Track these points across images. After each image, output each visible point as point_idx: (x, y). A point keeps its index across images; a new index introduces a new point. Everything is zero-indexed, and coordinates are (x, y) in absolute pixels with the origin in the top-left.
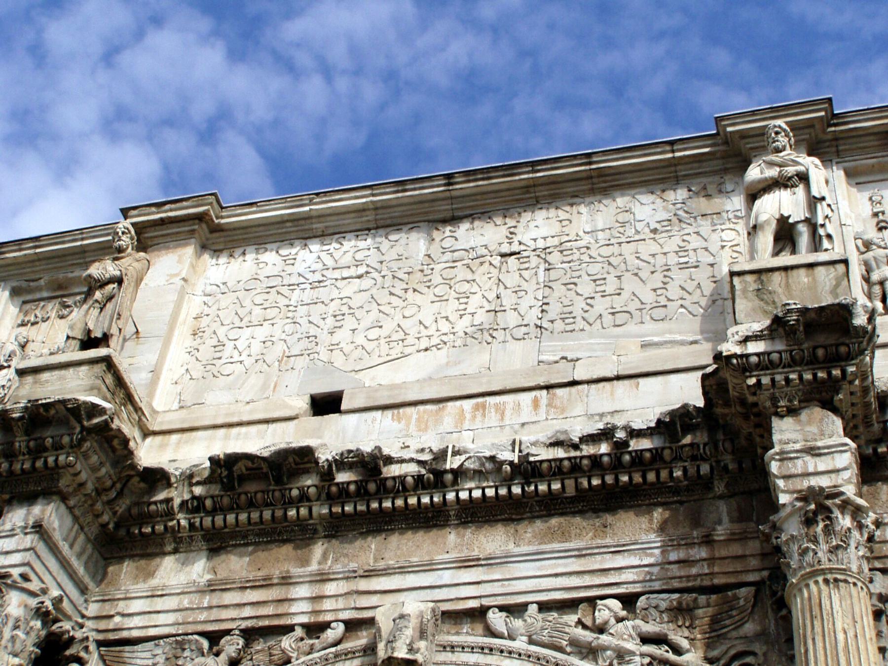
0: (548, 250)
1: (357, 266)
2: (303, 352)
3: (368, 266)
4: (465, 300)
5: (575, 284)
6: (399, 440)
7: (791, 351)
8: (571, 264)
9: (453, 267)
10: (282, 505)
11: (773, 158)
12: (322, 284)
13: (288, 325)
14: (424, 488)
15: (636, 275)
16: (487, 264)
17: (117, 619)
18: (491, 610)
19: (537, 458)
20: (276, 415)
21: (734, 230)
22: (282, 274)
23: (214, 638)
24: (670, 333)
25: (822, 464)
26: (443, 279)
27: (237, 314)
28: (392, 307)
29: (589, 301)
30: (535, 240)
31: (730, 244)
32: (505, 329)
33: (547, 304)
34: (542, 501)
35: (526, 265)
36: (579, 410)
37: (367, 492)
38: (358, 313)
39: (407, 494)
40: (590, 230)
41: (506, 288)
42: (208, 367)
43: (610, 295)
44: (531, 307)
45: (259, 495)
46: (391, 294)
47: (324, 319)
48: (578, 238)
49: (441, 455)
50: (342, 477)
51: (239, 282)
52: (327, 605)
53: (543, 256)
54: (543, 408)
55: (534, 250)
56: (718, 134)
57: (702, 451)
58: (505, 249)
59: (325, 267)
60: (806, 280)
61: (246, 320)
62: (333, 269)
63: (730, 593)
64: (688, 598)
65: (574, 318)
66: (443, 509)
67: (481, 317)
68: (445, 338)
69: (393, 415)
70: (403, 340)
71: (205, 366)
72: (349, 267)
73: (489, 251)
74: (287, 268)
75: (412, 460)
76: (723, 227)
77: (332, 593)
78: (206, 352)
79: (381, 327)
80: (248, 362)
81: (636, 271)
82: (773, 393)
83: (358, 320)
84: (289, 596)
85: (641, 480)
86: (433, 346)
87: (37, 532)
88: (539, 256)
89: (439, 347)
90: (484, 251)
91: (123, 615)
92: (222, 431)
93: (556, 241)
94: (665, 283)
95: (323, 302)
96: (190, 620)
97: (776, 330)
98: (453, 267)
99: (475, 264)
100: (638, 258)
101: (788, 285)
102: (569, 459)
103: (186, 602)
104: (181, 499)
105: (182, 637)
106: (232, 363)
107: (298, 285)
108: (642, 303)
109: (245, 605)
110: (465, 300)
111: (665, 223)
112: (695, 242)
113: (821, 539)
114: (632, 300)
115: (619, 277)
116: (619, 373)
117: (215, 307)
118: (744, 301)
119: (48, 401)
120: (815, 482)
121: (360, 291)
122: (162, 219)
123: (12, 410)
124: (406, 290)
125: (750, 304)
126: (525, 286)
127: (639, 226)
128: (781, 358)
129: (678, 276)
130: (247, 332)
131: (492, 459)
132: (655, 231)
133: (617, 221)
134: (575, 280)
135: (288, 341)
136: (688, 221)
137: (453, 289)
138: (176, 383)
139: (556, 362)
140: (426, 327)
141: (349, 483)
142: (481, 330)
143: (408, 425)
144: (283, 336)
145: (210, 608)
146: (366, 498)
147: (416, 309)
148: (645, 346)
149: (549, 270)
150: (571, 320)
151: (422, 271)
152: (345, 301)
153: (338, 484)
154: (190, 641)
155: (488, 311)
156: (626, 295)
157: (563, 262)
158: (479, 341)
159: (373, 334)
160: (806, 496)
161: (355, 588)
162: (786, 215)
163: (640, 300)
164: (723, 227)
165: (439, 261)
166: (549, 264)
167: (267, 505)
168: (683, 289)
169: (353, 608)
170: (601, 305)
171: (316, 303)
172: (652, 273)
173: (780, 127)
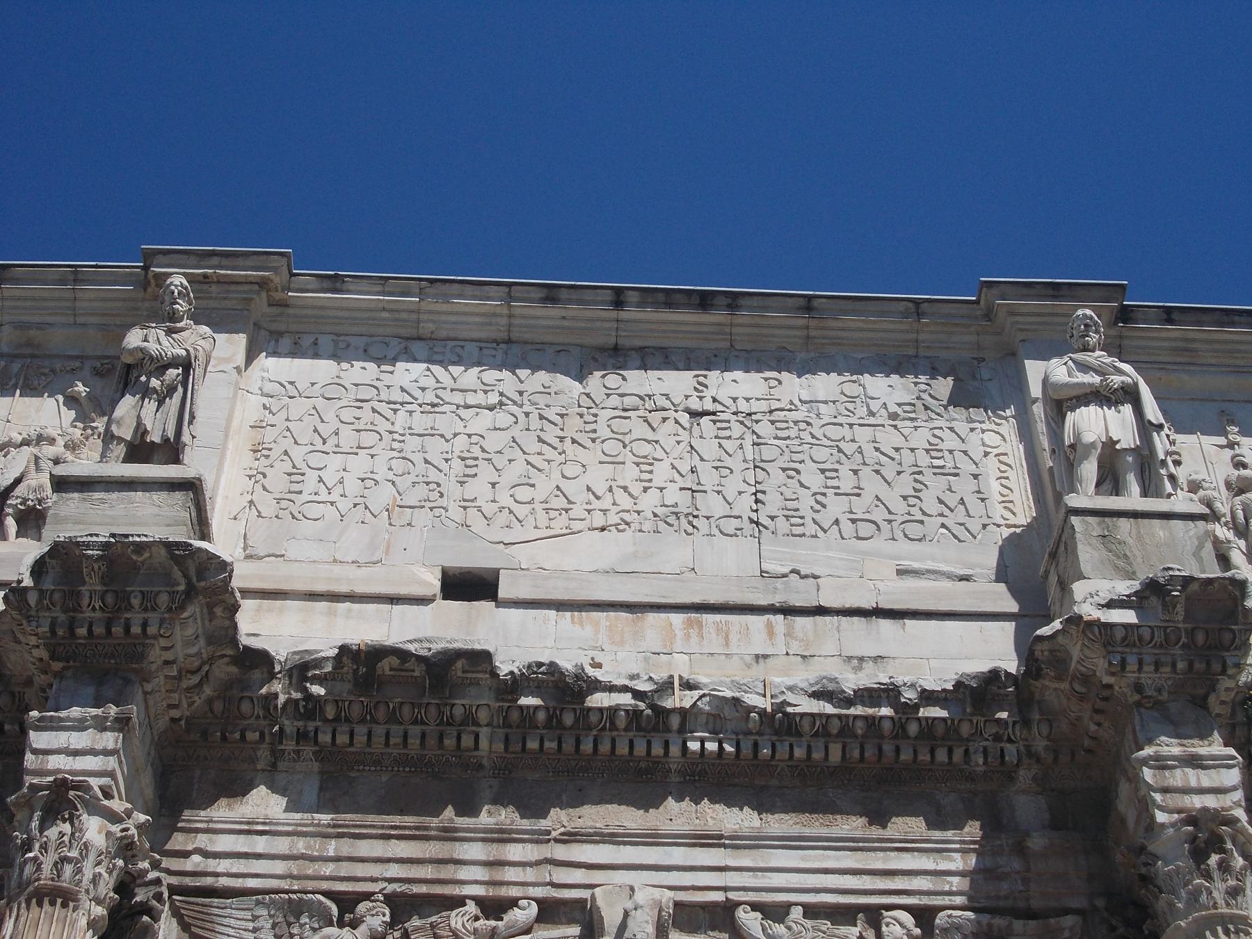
0: (754, 417)
3: (501, 394)
4: (648, 468)
5: (798, 472)
6: (586, 652)
7: (1166, 628)
8: (788, 442)
10: (437, 725)
11: (1079, 356)
12: (437, 409)
13: (394, 460)
14: (639, 729)
15: (877, 472)
16: (672, 421)
17: (196, 858)
18: (743, 906)
19: (798, 710)
20: (403, 591)
21: (998, 433)
23: (347, 904)
24: (933, 560)
25: (1207, 779)
26: (612, 431)
27: (316, 430)
28: (544, 460)
29: (819, 498)
30: (735, 400)
31: (995, 451)
32: (708, 518)
33: (764, 492)
34: (797, 767)
35: (727, 433)
36: (830, 648)
38: (496, 458)
39: (615, 733)
40: (808, 399)
41: (702, 459)
42: (284, 504)
43: (847, 495)
44: (740, 493)
45: (406, 710)
46: (540, 440)
47: (447, 460)
48: (793, 407)
49: (666, 687)
50: (527, 701)
51: (313, 384)
52: (511, 874)
53: (748, 423)
54: (780, 639)
55: (734, 413)
56: (977, 302)
57: (1010, 730)
58: (695, 404)
59: (439, 385)
60: (1161, 533)
61: (332, 442)
63: (1052, 921)
64: (999, 922)
65: (802, 518)
66: (662, 760)
67: (673, 495)
68: (626, 516)
69: (572, 617)
70: (567, 511)
71: (279, 500)
72: (475, 391)
73: (673, 403)
75: (625, 689)
76: (984, 426)
77: (517, 858)
78: (277, 479)
79: (533, 486)
80: (344, 505)
81: (877, 467)
82: (1139, 678)
83: (497, 470)
84: (455, 856)
85: (928, 758)
86: (611, 526)
87: (120, 730)
88: (742, 423)
90: (667, 404)
91: (206, 854)
92: (323, 605)
93: (763, 406)
94: (916, 490)
95: (442, 436)
96: (310, 872)
97: (1146, 598)
99: (655, 418)
100: (877, 449)
101: (1139, 537)
102: (839, 717)
103: (301, 845)
104: (286, 696)
105: (299, 895)
106: (319, 503)
107: (402, 404)
108: (890, 512)
109: (389, 860)
110: (648, 468)
111: (908, 408)
112: (950, 442)
113: (1216, 875)
114: (877, 506)
115: (855, 472)
116: (880, 606)
117: (283, 415)
118: (1088, 549)
119: (144, 539)
120: (1197, 802)
121: (496, 429)
122: (205, 276)
123: (88, 545)
124: (562, 439)
125: (1096, 554)
126: (728, 462)
127: (875, 406)
128: (1153, 633)
129: (936, 486)
130: (335, 461)
131: (736, 701)
132: (894, 416)
133: (842, 393)
134: (796, 465)
136: (938, 411)
137: (628, 448)
138: (235, 519)
139: (784, 576)
140: (598, 498)
141: (537, 708)
142: (676, 514)
143: (597, 632)
144: (390, 476)
145: (337, 859)
146: (558, 732)
147: (580, 469)
148: (901, 572)
149: (758, 444)
150: (800, 521)
152: (475, 439)
155: (681, 489)
156: (868, 498)
157: (776, 438)
158: (676, 528)
159: (524, 493)
160: (1193, 819)
161: (549, 856)
162: (1115, 439)
163: (887, 508)
164: (984, 426)
166: (759, 437)
168: (941, 502)
170: (836, 507)
172: (899, 473)
173: (1091, 318)
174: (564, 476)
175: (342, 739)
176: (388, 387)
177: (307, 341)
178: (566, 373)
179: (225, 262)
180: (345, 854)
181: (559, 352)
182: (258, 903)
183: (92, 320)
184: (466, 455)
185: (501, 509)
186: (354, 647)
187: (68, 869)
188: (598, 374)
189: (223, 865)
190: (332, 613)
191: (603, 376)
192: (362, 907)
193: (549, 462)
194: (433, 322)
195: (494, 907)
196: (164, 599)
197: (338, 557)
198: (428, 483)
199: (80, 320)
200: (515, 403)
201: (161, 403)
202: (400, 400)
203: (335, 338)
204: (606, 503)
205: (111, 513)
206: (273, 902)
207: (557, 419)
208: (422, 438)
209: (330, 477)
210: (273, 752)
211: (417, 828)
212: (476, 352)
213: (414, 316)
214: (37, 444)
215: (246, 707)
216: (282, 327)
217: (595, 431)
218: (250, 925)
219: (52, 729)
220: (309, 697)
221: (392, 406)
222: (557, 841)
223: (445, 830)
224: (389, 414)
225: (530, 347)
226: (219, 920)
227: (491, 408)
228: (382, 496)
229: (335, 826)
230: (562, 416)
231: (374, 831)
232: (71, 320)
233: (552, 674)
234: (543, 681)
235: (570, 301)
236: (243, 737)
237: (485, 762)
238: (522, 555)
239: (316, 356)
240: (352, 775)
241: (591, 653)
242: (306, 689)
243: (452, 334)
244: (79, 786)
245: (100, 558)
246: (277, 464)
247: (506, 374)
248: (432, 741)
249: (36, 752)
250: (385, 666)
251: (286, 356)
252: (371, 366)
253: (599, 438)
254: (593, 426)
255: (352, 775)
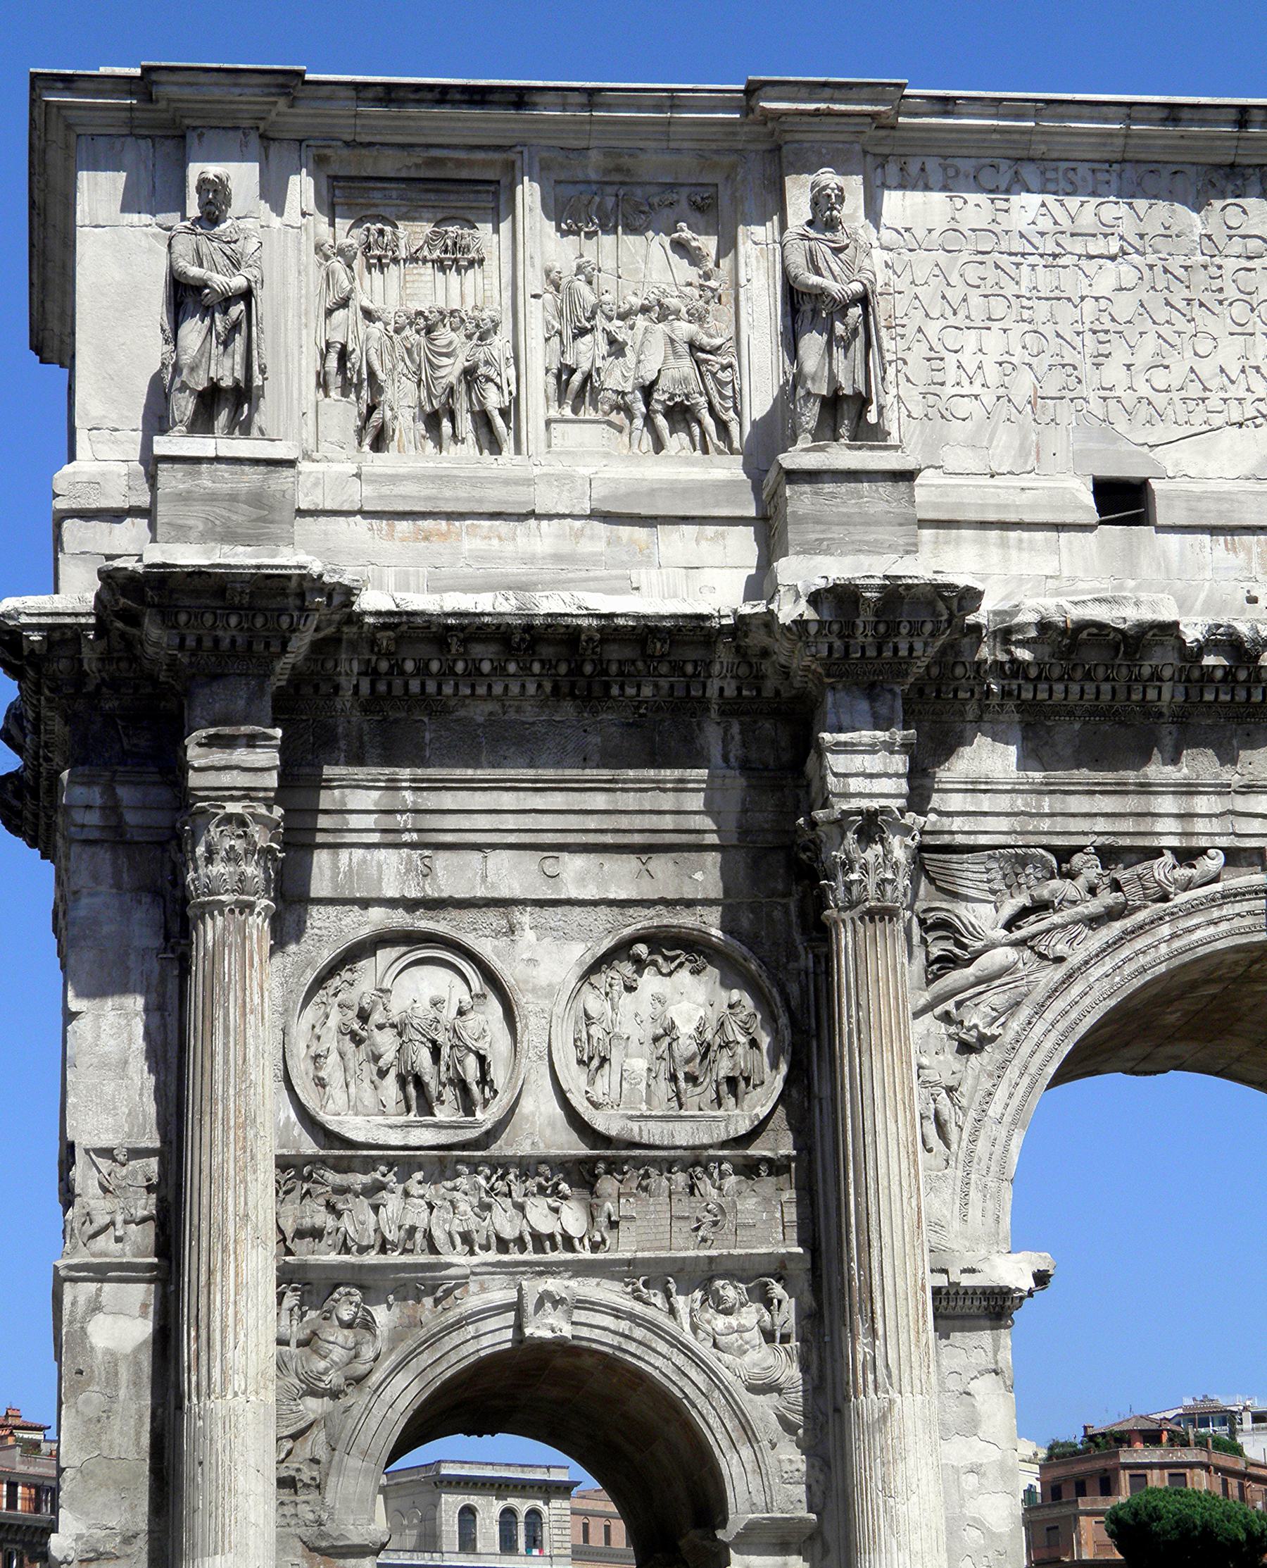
1: (1106, 236)
2: (1064, 393)
3: (1122, 238)
9: (1250, 270)
12: (1060, 261)
20: (1069, 518)
22: (994, 227)
23: (1064, 854)
27: (944, 297)
37: (1235, 681)
45: (1101, 672)
46: (1168, 303)
50: (1209, 660)
51: (930, 231)
52: (1200, 825)
61: (962, 313)
62: (1072, 235)
69: (1226, 541)
71: (924, 395)
72: (1094, 235)
74: (1001, 216)
79: (1167, 367)
80: (988, 398)
87: (906, 753)
89: (1258, 421)
91: (941, 813)
92: (994, 534)
95: (1069, 299)
96: (1030, 828)
98: (1250, 270)
103: (1020, 803)
107: (1023, 255)
109: (1096, 815)
117: (907, 277)
119: (916, 581)
121: (1121, 289)
122: (818, 110)
123: (867, 588)
135: (1034, 366)
140: (1233, 382)
141: (1214, 667)
145: (1052, 815)
147: (1211, 343)
151: (1205, 267)
153: (1202, 667)
154: (1034, 856)
161: (1231, 808)
165: (1225, 252)
167: (1107, 679)
169: (1231, 834)
171: (1059, 299)
174: (1196, 354)
175: (1041, 696)
176: (1007, 232)
177: (914, 167)
178: (1184, 203)
179: (837, 94)
180: (1058, 811)
181: (1176, 173)
182: (990, 857)
183: (686, 145)
184: (1097, 327)
185: (1140, 400)
186: (1062, 625)
187: (889, 888)
188: (1218, 204)
189: (957, 824)
190: (1004, 544)
191: (1224, 208)
192: (1077, 859)
193: (1179, 333)
194: (1045, 142)
195: (1187, 856)
196: (928, 628)
197: (995, 469)
198: (1064, 366)
199: (673, 145)
200: (1137, 252)
201: (846, 349)
202: (1021, 250)
203: (942, 161)
204: (1242, 393)
205: (845, 510)
206: (1002, 855)
207: (1180, 272)
208: (1050, 302)
209: (971, 368)
210: (980, 706)
211: (1118, 784)
212: (1089, 175)
213: (1026, 137)
214: (662, 318)
215: (959, 671)
216: (886, 151)
217: (1221, 290)
218: (985, 877)
219: (846, 752)
220: (1014, 661)
221: (1013, 259)
222: (1236, 792)
223: (1141, 785)
224: (1012, 270)
225: (1144, 167)
226: (958, 873)
227: (1113, 258)
228: (1023, 384)
229: (1047, 784)
230: (1186, 268)
231: (1080, 788)
232: (664, 144)
233: (1231, 635)
234: (1220, 640)
235: (1192, 122)
236: (955, 695)
237: (1165, 710)
238: (1168, 458)
239: (927, 188)
240: (1049, 723)
241: (1247, 585)
242: (1009, 652)
243: (1064, 156)
244: (884, 811)
245: (879, 599)
246: (915, 346)
247: (1123, 210)
248: (1122, 696)
249: (836, 775)
250: (1084, 635)
251: (896, 188)
252: (982, 198)
253: (1226, 299)
254: (1217, 284)
255: (1049, 723)
